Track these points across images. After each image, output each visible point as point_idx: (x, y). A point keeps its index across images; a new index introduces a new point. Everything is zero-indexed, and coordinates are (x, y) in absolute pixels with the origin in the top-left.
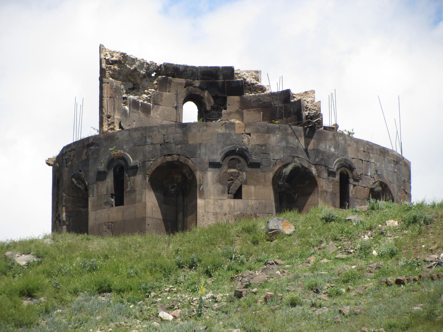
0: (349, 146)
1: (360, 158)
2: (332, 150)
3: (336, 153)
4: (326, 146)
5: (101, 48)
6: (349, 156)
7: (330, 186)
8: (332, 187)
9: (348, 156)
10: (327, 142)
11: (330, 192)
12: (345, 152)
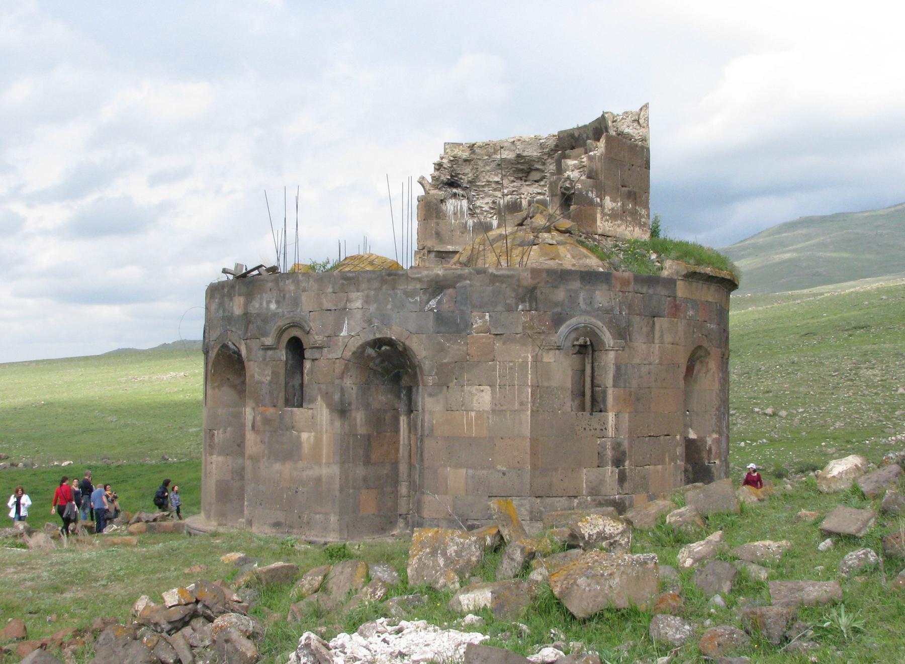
0: (304, 290)
1: (325, 307)
2: (273, 306)
3: (280, 310)
4: (261, 304)
5: (646, 106)
6: (304, 308)
7: (266, 372)
8: (270, 373)
9: (301, 310)
10: (264, 295)
11: (267, 382)
12: (296, 302)
